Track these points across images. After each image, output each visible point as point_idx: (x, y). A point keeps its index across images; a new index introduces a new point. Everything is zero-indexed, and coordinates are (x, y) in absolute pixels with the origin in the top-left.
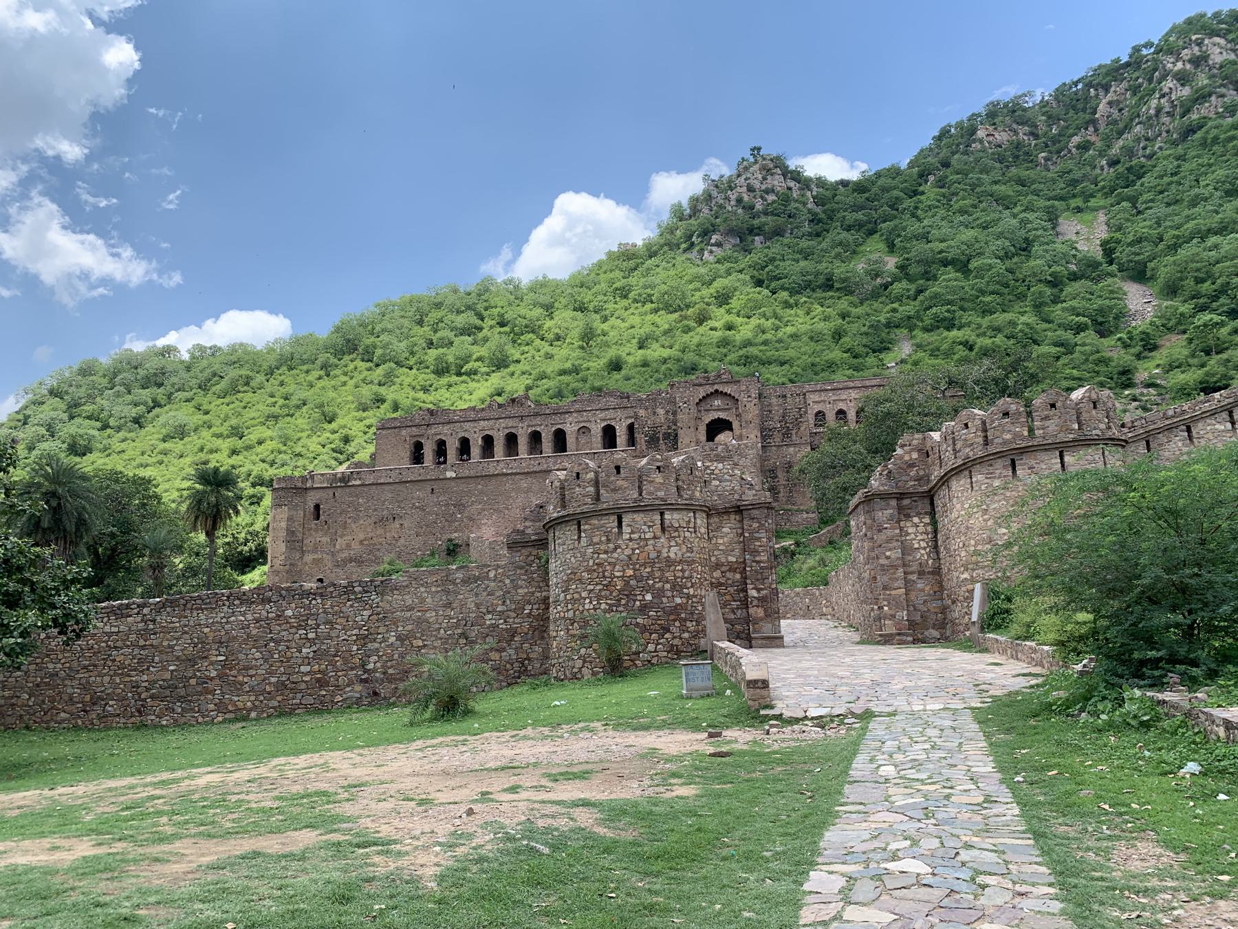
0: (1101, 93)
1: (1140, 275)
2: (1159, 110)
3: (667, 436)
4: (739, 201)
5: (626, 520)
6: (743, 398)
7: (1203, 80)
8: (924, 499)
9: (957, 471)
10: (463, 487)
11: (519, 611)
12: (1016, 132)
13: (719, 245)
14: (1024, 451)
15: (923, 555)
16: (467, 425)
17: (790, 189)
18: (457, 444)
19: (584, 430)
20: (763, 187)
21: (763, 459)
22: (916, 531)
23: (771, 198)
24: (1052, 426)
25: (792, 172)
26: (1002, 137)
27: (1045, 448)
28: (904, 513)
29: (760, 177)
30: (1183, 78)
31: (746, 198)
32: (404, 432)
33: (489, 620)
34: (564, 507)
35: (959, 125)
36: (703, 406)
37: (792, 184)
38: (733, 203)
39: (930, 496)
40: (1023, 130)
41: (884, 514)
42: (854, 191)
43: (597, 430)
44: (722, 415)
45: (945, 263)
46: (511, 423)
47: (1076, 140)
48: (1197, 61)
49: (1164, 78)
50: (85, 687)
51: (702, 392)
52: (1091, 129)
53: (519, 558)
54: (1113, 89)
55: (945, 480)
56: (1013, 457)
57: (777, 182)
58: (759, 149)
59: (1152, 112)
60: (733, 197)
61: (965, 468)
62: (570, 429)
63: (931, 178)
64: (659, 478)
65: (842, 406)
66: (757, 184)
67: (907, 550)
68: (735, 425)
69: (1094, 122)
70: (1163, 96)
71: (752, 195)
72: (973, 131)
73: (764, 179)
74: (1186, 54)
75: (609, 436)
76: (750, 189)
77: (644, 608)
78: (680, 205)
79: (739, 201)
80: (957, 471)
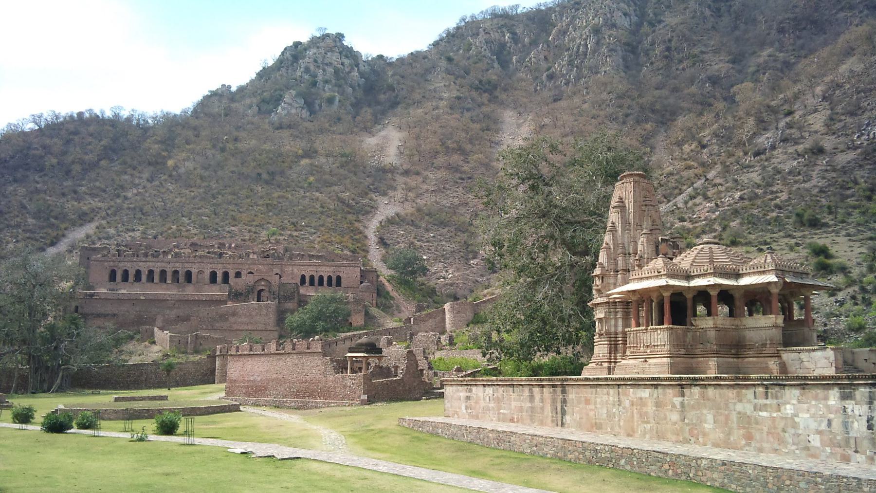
12: (504, 36)
16: (141, 264)
17: (342, 64)
46: (164, 264)
57: (334, 58)
62: (194, 271)
66: (320, 60)
75: (213, 275)
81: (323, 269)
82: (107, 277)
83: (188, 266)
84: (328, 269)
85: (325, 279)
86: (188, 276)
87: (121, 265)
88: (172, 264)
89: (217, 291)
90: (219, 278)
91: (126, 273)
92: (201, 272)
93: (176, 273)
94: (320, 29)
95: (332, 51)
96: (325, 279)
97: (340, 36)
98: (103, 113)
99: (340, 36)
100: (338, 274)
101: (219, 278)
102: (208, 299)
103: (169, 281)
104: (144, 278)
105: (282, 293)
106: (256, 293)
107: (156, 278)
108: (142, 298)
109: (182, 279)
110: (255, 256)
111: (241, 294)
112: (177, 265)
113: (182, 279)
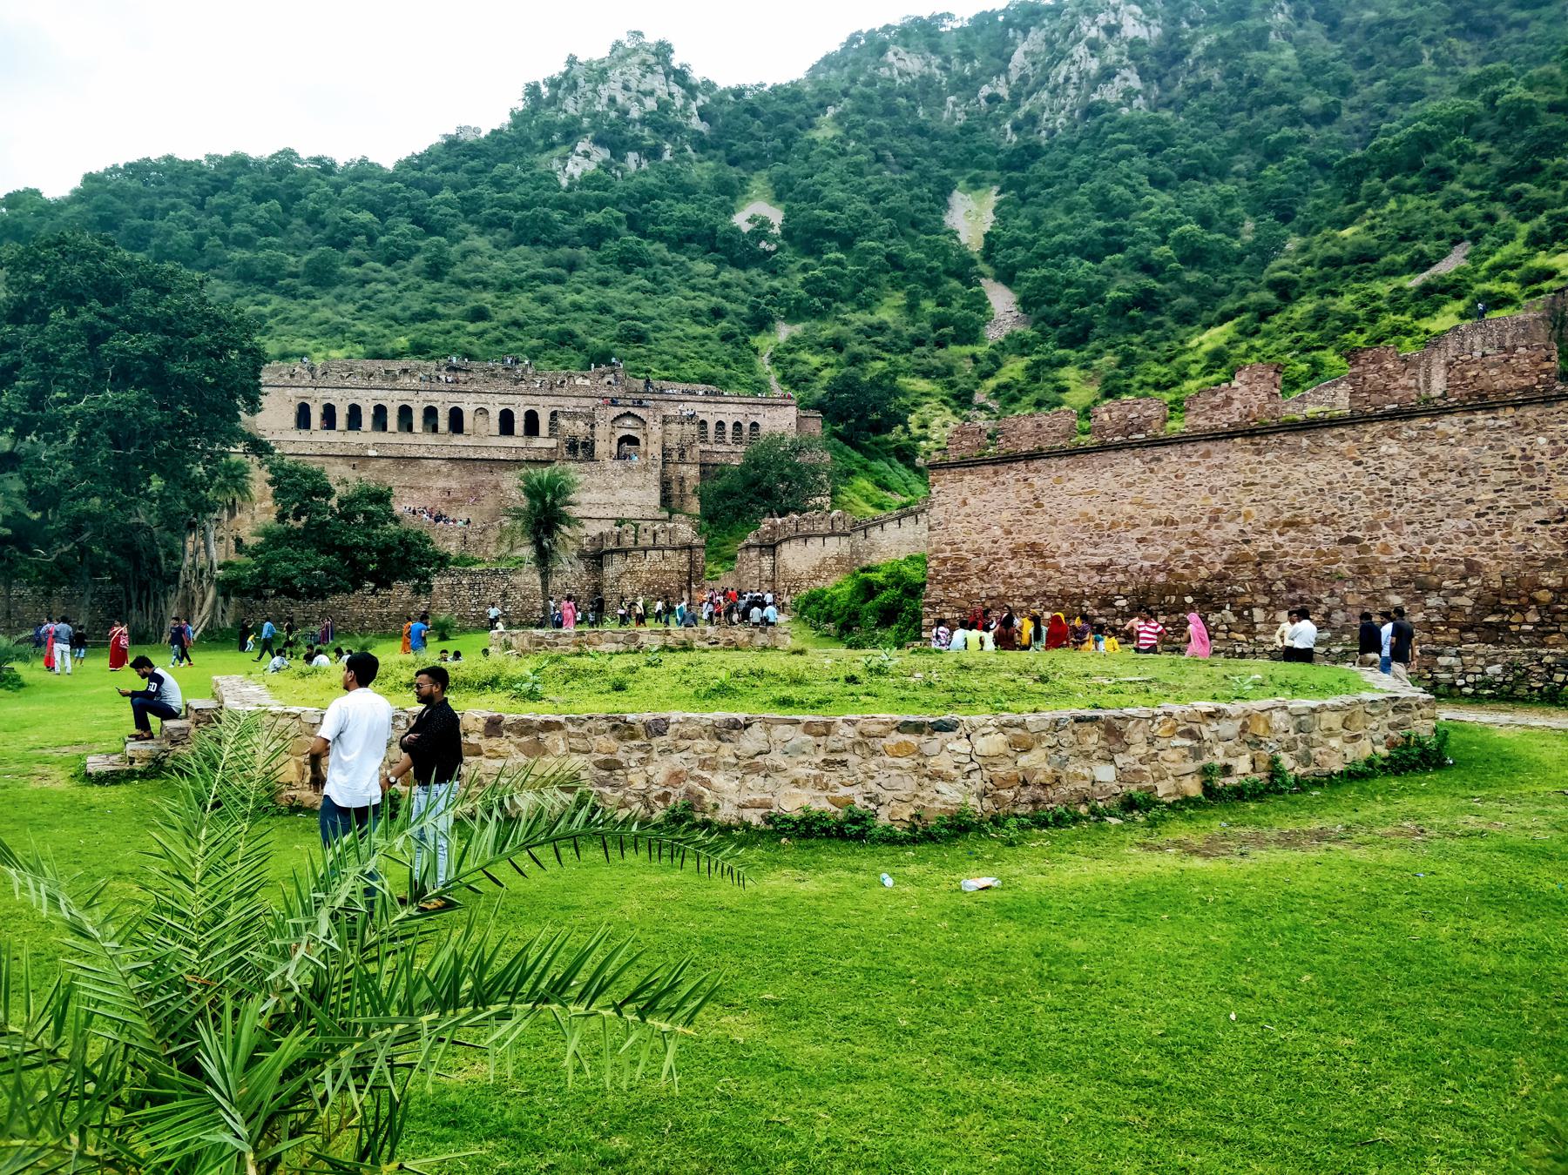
0: (1020, 34)
2: (1067, 79)
3: (584, 445)
4: (612, 100)
6: (650, 422)
7: (1111, 54)
10: (383, 463)
11: (583, 588)
12: (929, 65)
13: (587, 155)
15: (768, 573)
17: (670, 94)
19: (483, 411)
20: (642, 88)
21: (663, 474)
22: (766, 562)
23: (651, 104)
24: (822, 527)
25: (676, 72)
26: (914, 65)
28: (762, 554)
29: (638, 72)
30: (1094, 47)
31: (620, 99)
32: (289, 392)
35: (871, 34)
36: (618, 424)
37: (675, 89)
38: (604, 101)
39: (774, 547)
40: (937, 60)
41: (753, 554)
42: (746, 111)
43: (495, 414)
44: (632, 433)
45: (830, 235)
46: (405, 395)
47: (986, 90)
48: (1111, 30)
49: (1077, 40)
51: (617, 411)
52: (1003, 78)
54: (1031, 35)
55: (780, 543)
57: (657, 82)
58: (640, 34)
59: (1061, 80)
60: (605, 94)
61: (788, 539)
62: (468, 406)
63: (831, 111)
65: (721, 418)
66: (633, 84)
67: (761, 570)
68: (642, 442)
70: (1074, 63)
71: (628, 94)
72: (882, 49)
73: (643, 76)
74: (1102, 19)
75: (506, 420)
76: (626, 88)
82: (291, 420)
85: (729, 428)
87: (320, 393)
90: (519, 426)
95: (653, 72)
96: (729, 428)
97: (663, 51)
100: (753, 419)
101: (519, 426)
103: (415, 429)
106: (615, 442)
107: (392, 421)
108: (372, 453)
109: (443, 424)
110: (587, 382)
112: (435, 396)
113: (443, 424)
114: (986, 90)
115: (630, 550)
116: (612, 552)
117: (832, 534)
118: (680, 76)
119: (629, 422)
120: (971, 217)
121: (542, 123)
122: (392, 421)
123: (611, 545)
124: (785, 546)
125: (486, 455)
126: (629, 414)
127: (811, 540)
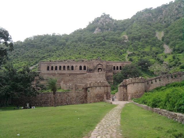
1: (168, 43)
5: (97, 88)
8: (125, 86)
9: (129, 84)
12: (150, 15)
14: (135, 83)
17: (110, 21)
18: (55, 67)
24: (137, 80)
27: (137, 83)
33: (80, 97)
34: (90, 85)
37: (111, 21)
41: (122, 88)
43: (78, 67)
44: (100, 67)
47: (159, 17)
50: (35, 102)
53: (83, 90)
55: (128, 85)
56: (134, 83)
62: (74, 66)
64: (100, 83)
66: (104, 20)
69: (162, 14)
75: (81, 67)
77: (98, 96)
78: (90, 22)
79: (101, 23)
80: (129, 84)
81: (118, 64)
82: (46, 69)
83: (72, 65)
84: (120, 64)
85: (119, 67)
86: (72, 67)
88: (67, 64)
89: (83, 71)
90: (83, 68)
91: (52, 67)
92: (76, 66)
93: (68, 67)
94: (103, 13)
95: (107, 18)
96: (119, 67)
97: (108, 15)
98: (50, 35)
99: (108, 15)
101: (83, 68)
102: (80, 73)
103: (66, 70)
104: (58, 69)
105: (107, 69)
106: (97, 69)
107: (62, 69)
108: (56, 73)
109: (70, 68)
111: (92, 70)
112: (69, 64)
113: (70, 68)
114: (159, 17)
115: (93, 87)
116: (89, 87)
117: (140, 82)
118: (111, 19)
119: (100, 65)
120: (160, 35)
121: (91, 28)
122: (62, 69)
123: (89, 86)
124: (129, 85)
125: (75, 73)
126: (99, 64)
127: (135, 84)
